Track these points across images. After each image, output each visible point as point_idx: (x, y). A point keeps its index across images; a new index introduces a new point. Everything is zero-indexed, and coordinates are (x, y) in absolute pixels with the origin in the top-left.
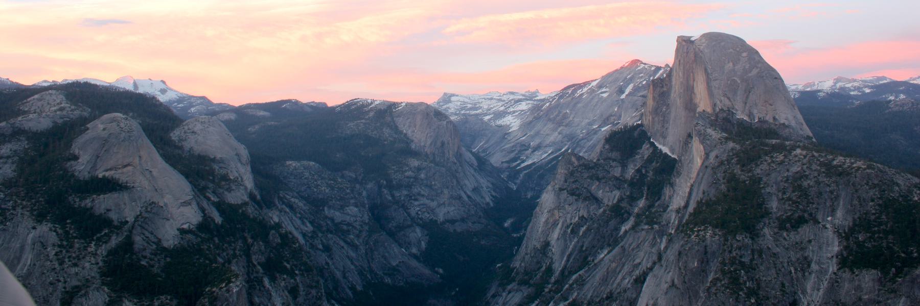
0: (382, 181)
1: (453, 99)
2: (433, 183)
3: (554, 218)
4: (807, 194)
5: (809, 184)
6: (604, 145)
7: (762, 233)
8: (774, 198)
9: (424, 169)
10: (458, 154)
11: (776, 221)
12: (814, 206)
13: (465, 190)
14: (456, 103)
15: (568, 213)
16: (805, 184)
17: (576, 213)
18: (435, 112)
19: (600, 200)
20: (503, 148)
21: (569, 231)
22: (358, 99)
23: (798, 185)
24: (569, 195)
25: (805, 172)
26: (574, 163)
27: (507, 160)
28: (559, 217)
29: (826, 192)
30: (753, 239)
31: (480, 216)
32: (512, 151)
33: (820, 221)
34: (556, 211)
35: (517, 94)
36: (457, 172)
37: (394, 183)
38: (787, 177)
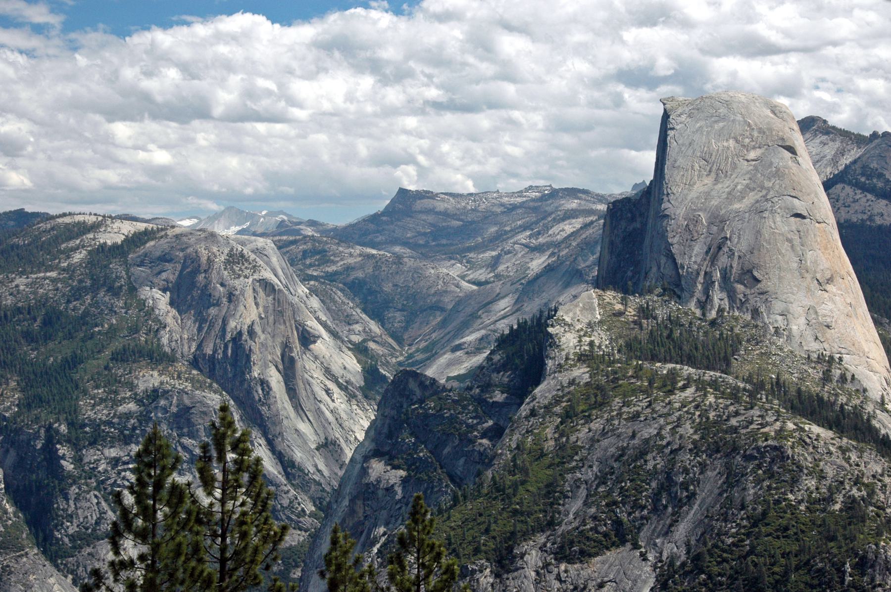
0: (56, 425)
1: (419, 205)
2: (185, 430)
3: (356, 519)
4: (641, 487)
5: (655, 466)
6: (492, 352)
7: (520, 563)
8: (583, 492)
9: (166, 392)
10: (286, 359)
11: (559, 539)
12: (645, 512)
13: (279, 448)
14: (424, 217)
15: (382, 508)
16: (650, 466)
17: (400, 508)
18: (231, 255)
19: (458, 481)
20: (457, 342)
21: (375, 550)
22: (70, 214)
23: (634, 467)
24: (389, 468)
25: (662, 438)
26: (412, 392)
27: (462, 372)
28: (366, 516)
29: (676, 483)
30: (497, 576)
31: (303, 510)
32: (478, 350)
33: (643, 544)
34: (359, 503)
35: (583, 196)
36: (263, 404)
37: (87, 429)
38: (623, 449)
